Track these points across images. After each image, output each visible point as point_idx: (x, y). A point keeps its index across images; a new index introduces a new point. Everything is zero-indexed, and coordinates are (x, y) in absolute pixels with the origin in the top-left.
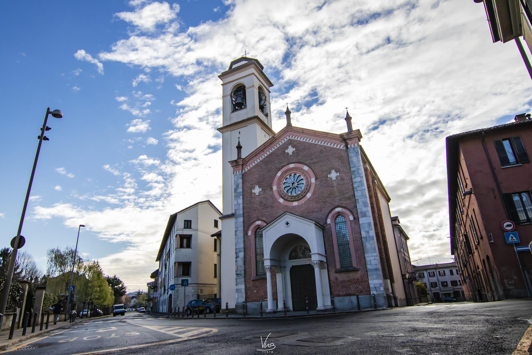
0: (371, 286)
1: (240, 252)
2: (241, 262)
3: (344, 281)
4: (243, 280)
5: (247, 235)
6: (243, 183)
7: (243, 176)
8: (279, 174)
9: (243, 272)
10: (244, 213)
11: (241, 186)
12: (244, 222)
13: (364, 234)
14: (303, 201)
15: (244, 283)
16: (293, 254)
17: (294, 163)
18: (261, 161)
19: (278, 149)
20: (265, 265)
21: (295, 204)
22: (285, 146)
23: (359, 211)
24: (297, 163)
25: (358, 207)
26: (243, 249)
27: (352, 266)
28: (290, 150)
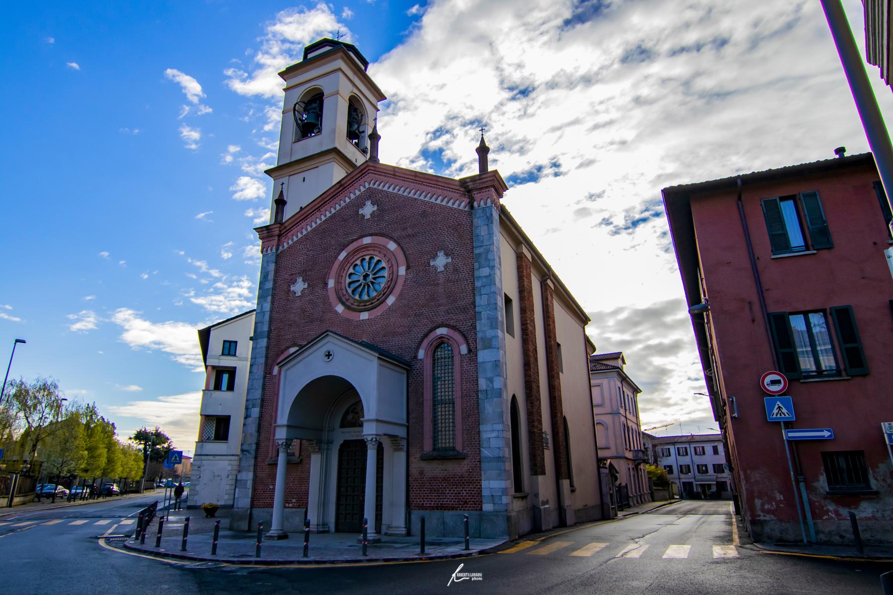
0: (485, 493)
1: (254, 406)
2: (253, 428)
3: (435, 478)
4: (252, 462)
5: (271, 373)
6: (276, 271)
7: (279, 257)
8: (342, 256)
9: (254, 446)
10: (270, 331)
11: (271, 276)
12: (267, 348)
13: (483, 383)
14: (378, 312)
15: (252, 468)
16: (350, 417)
17: (371, 235)
18: (314, 230)
19: (347, 207)
20: (277, 436)
21: (364, 316)
22: (359, 203)
23: (479, 335)
24: (376, 235)
25: (478, 328)
26: (259, 401)
28: (368, 210)
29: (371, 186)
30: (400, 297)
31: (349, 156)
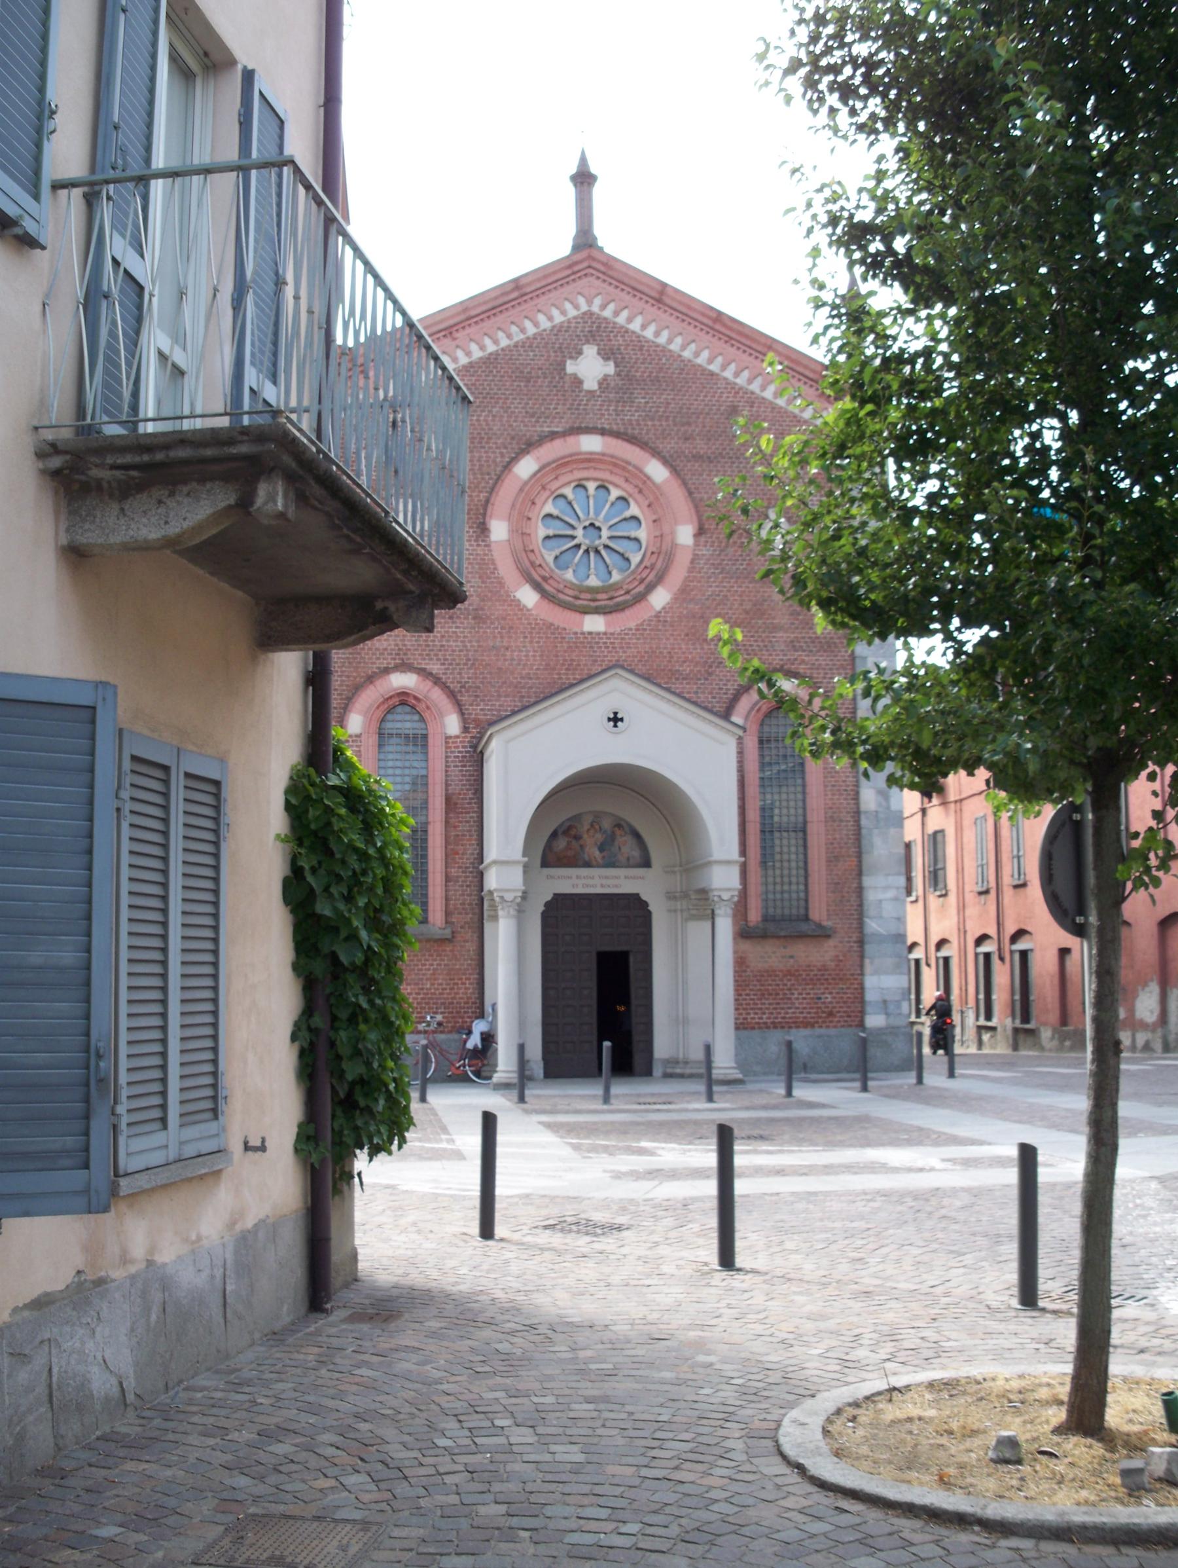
0: (870, 996)
3: (771, 973)
8: (526, 467)
14: (629, 620)
17: (603, 432)
19: (528, 344)
21: (594, 624)
22: (565, 342)
24: (617, 435)
27: (806, 918)
28: (590, 368)
29: (595, 309)
30: (683, 594)
31: (1075, 1256)
